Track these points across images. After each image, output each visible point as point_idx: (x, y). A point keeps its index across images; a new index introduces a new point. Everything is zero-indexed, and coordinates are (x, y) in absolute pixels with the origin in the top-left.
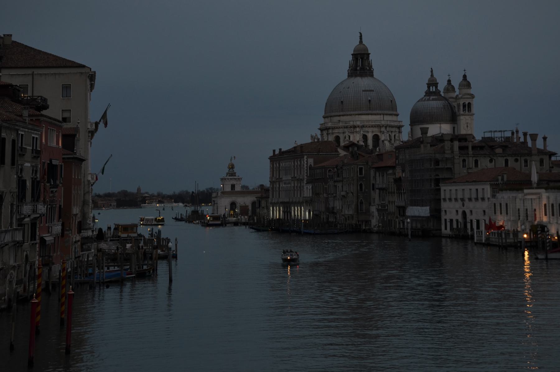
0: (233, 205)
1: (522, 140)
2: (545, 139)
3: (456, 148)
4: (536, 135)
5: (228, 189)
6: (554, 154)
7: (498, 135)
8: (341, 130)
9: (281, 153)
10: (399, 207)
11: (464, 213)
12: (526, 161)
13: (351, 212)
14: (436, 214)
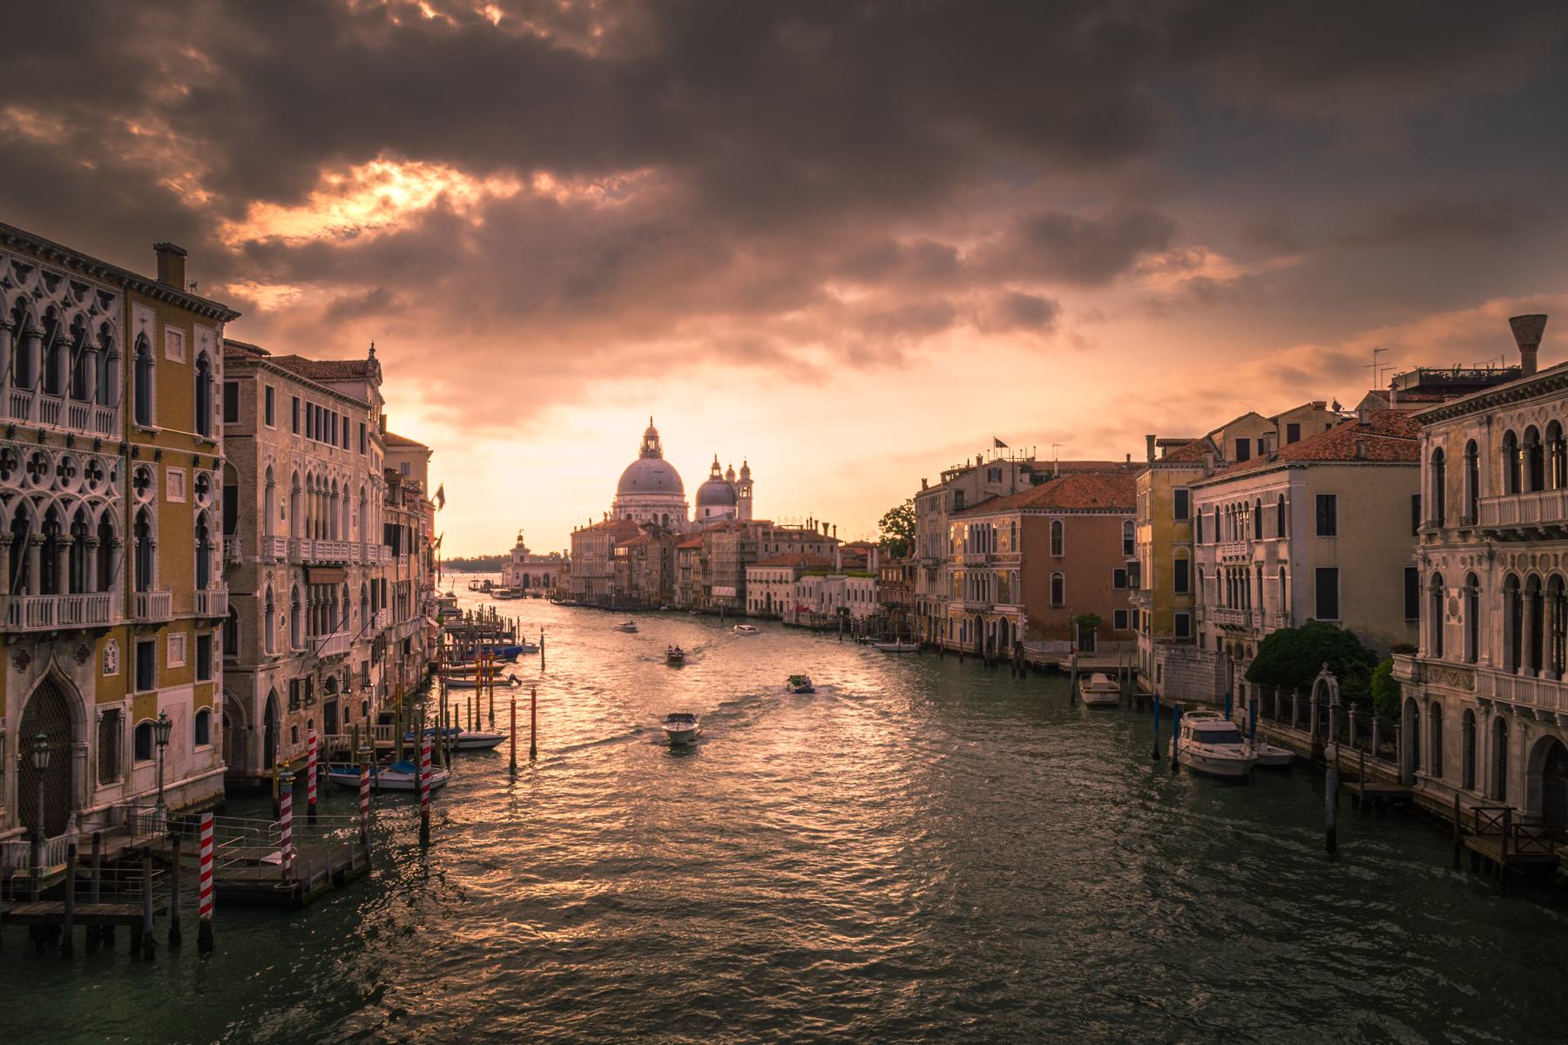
0: (526, 576)
2: (835, 527)
3: (760, 534)
8: (633, 509)
9: (583, 530)
10: (704, 587)
11: (768, 595)
12: (819, 547)
14: (742, 594)
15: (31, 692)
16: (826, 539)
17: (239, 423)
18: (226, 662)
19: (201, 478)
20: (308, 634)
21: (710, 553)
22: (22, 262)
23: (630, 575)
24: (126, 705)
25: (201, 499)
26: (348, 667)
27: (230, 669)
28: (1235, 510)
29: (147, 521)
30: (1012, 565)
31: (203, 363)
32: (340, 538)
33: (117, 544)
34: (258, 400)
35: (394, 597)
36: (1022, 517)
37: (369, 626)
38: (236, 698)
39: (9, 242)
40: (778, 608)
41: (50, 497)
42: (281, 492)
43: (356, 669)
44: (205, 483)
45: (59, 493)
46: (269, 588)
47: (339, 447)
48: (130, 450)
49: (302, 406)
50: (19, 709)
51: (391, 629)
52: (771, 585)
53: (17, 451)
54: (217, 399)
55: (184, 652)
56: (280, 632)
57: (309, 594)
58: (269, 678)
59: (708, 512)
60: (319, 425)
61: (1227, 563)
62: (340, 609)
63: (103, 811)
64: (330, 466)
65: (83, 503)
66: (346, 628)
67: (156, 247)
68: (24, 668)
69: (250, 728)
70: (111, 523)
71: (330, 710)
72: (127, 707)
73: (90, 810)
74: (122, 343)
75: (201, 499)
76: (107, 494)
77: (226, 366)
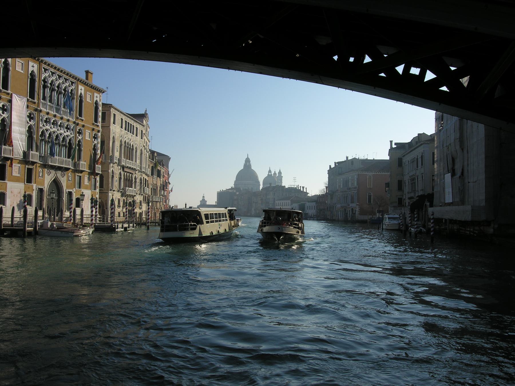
2: (306, 188)
4: (304, 187)
15: (51, 182)
19: (94, 135)
22: (53, 71)
24: (73, 191)
25: (95, 140)
28: (412, 161)
30: (354, 190)
31: (96, 103)
36: (358, 175)
42: (117, 144)
43: (138, 201)
46: (113, 170)
47: (135, 135)
53: (49, 119)
54: (100, 114)
56: (116, 184)
61: (411, 178)
64: (132, 140)
66: (135, 188)
69: (106, 208)
75: (95, 140)
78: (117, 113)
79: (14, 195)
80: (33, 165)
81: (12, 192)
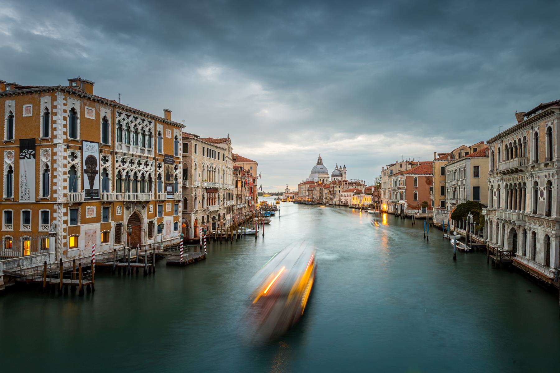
1: (359, 182)
2: (364, 182)
3: (344, 184)
5: (286, 192)
6: (366, 185)
7: (354, 180)
9: (301, 184)
12: (360, 187)
13: (318, 199)
15: (130, 216)
16: (362, 185)
17: (188, 153)
18: (183, 211)
19: (176, 166)
20: (207, 205)
21: (331, 189)
22: (128, 114)
23: (312, 195)
24: (155, 220)
25: (176, 171)
26: (219, 214)
27: (184, 213)
29: (161, 176)
31: (176, 138)
32: (217, 182)
33: (153, 181)
34: (192, 147)
35: (236, 198)
37: (225, 203)
38: (187, 220)
39: (124, 110)
40: (348, 203)
41: (135, 170)
43: (222, 214)
44: (177, 167)
45: (137, 169)
48: (156, 159)
49: (205, 149)
50: (127, 219)
51: (234, 206)
52: (347, 197)
55: (171, 208)
57: (207, 195)
58: (195, 215)
59: (334, 178)
60: (210, 154)
62: (217, 199)
63: (149, 245)
65: (143, 171)
67: (164, 110)
68: (128, 210)
69: (190, 227)
70: (151, 176)
71: (214, 224)
72: (155, 220)
73: (145, 244)
74: (154, 133)
75: (176, 171)
76: (150, 169)
77: (183, 139)
78: (197, 143)
79: (89, 236)
80: (110, 204)
81: (86, 233)
